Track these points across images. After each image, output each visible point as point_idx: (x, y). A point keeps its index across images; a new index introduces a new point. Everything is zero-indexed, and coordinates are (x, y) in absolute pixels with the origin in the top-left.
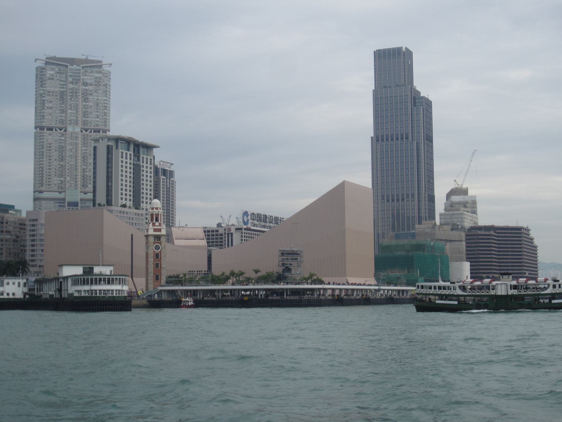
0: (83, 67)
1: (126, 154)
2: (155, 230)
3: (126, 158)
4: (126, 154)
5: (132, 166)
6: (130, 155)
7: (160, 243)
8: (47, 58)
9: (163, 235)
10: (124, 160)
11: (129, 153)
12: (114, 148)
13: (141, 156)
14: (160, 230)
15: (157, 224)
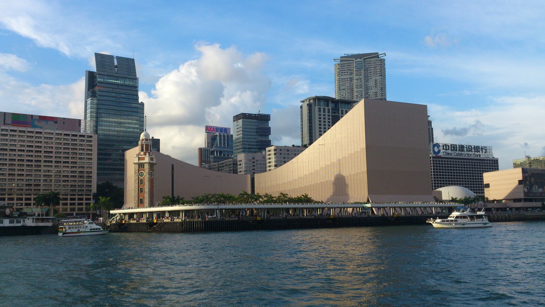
0: (364, 59)
1: (324, 109)
2: (139, 159)
3: (324, 112)
4: (324, 109)
5: (331, 117)
6: (329, 109)
7: (144, 170)
8: (341, 57)
9: (145, 163)
10: (322, 113)
11: (326, 108)
12: (313, 106)
13: (340, 110)
14: (143, 159)
15: (142, 153)
